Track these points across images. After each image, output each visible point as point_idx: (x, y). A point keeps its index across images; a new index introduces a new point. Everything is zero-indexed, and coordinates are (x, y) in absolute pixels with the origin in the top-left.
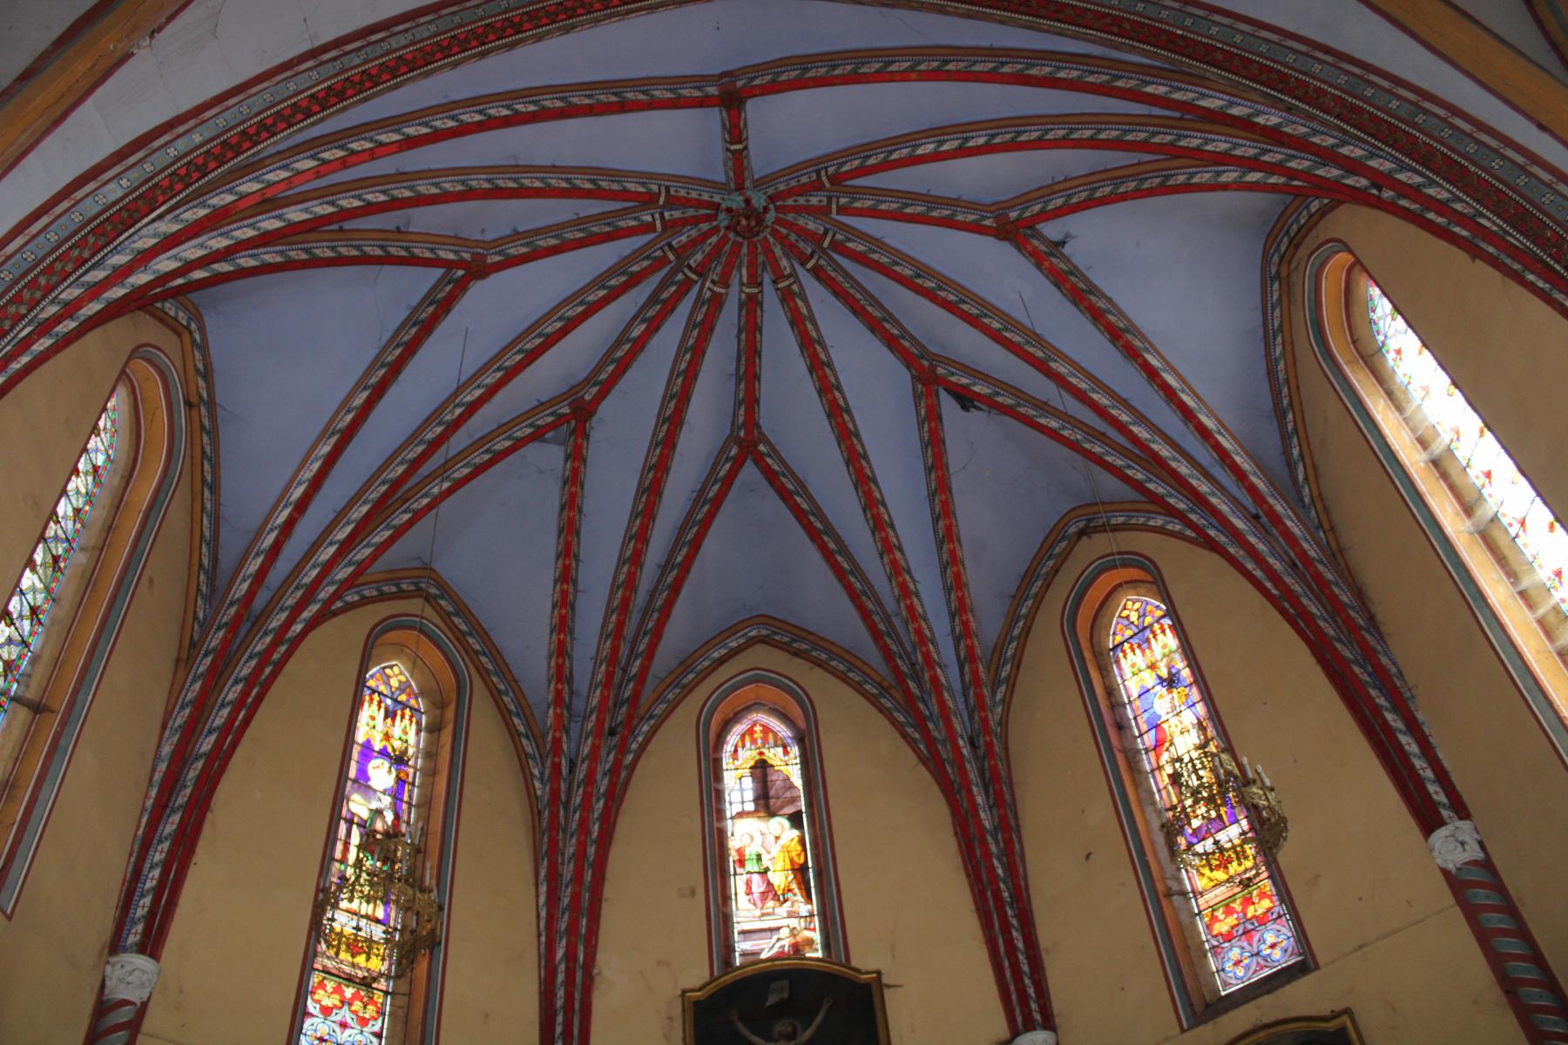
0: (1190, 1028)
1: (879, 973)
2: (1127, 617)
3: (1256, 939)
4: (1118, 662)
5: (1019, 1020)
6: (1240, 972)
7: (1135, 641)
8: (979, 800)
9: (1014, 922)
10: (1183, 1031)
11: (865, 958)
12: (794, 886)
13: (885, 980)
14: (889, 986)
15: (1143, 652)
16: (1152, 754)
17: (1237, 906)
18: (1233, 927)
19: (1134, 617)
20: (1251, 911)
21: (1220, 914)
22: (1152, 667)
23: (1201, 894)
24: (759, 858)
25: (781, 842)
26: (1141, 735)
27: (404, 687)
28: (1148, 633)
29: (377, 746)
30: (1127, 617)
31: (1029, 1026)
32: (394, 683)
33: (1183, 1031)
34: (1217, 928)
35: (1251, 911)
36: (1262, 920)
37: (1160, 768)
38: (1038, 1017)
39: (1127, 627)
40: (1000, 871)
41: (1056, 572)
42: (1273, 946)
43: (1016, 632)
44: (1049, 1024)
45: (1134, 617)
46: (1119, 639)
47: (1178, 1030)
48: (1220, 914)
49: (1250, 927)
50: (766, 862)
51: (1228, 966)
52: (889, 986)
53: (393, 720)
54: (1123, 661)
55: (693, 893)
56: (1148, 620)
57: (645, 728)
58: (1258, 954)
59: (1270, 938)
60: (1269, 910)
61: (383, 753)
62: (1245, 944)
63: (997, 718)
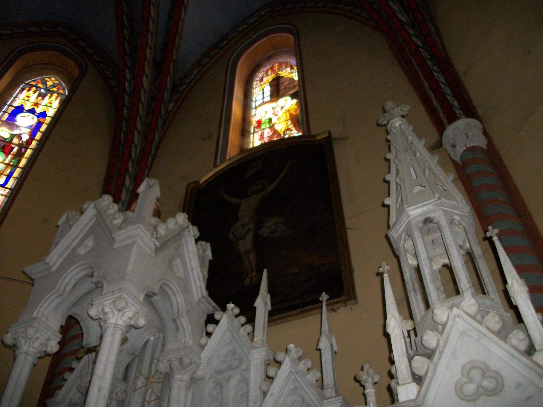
1: (330, 134)
11: (319, 131)
12: (291, 126)
13: (333, 136)
14: (339, 139)
24: (270, 120)
25: (284, 109)
27: (54, 86)
29: (28, 107)
32: (49, 83)
50: (274, 121)
52: (339, 139)
53: (43, 99)
55: (210, 136)
57: (195, 72)
61: (32, 111)
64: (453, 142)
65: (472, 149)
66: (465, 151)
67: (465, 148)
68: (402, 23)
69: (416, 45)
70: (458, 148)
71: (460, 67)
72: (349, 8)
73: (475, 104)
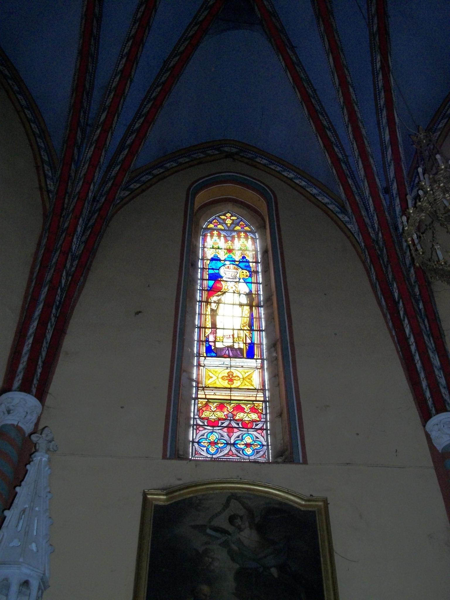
0: (170, 458)
2: (224, 220)
3: (235, 435)
4: (205, 236)
5: (17, 384)
6: (212, 450)
7: (223, 233)
8: (79, 229)
9: (53, 319)
10: (164, 457)
15: (226, 241)
16: (205, 294)
17: (230, 408)
18: (220, 419)
19: (229, 222)
20: (240, 416)
21: (213, 407)
22: (230, 251)
23: (204, 388)
26: (202, 279)
28: (234, 234)
30: (224, 220)
31: (25, 388)
33: (164, 457)
34: (206, 414)
35: (240, 416)
36: (245, 426)
37: (207, 302)
38: (34, 390)
39: (220, 224)
40: (63, 282)
41: (201, 163)
42: (248, 445)
43: (155, 172)
44: (41, 395)
45: (229, 222)
46: (211, 226)
47: (161, 457)
48: (213, 407)
49: (234, 425)
51: (205, 443)
54: (209, 238)
56: (238, 228)
58: (234, 444)
59: (248, 440)
60: (253, 421)
62: (225, 434)
63: (121, 195)
64: (11, 408)
65: (18, 429)
66: (13, 425)
67: (16, 423)
68: (70, 248)
69: (60, 282)
70: (10, 417)
71: (69, 343)
72: (46, 158)
73: (51, 390)
